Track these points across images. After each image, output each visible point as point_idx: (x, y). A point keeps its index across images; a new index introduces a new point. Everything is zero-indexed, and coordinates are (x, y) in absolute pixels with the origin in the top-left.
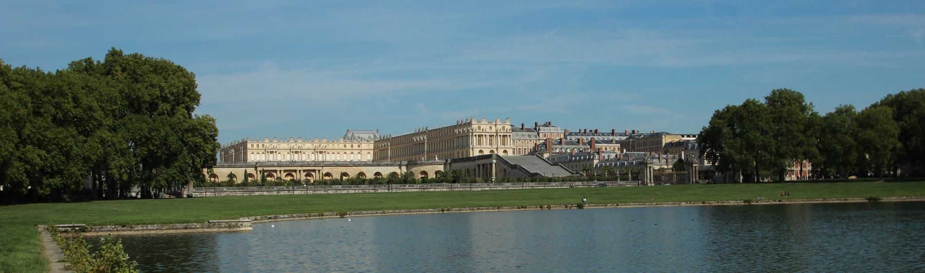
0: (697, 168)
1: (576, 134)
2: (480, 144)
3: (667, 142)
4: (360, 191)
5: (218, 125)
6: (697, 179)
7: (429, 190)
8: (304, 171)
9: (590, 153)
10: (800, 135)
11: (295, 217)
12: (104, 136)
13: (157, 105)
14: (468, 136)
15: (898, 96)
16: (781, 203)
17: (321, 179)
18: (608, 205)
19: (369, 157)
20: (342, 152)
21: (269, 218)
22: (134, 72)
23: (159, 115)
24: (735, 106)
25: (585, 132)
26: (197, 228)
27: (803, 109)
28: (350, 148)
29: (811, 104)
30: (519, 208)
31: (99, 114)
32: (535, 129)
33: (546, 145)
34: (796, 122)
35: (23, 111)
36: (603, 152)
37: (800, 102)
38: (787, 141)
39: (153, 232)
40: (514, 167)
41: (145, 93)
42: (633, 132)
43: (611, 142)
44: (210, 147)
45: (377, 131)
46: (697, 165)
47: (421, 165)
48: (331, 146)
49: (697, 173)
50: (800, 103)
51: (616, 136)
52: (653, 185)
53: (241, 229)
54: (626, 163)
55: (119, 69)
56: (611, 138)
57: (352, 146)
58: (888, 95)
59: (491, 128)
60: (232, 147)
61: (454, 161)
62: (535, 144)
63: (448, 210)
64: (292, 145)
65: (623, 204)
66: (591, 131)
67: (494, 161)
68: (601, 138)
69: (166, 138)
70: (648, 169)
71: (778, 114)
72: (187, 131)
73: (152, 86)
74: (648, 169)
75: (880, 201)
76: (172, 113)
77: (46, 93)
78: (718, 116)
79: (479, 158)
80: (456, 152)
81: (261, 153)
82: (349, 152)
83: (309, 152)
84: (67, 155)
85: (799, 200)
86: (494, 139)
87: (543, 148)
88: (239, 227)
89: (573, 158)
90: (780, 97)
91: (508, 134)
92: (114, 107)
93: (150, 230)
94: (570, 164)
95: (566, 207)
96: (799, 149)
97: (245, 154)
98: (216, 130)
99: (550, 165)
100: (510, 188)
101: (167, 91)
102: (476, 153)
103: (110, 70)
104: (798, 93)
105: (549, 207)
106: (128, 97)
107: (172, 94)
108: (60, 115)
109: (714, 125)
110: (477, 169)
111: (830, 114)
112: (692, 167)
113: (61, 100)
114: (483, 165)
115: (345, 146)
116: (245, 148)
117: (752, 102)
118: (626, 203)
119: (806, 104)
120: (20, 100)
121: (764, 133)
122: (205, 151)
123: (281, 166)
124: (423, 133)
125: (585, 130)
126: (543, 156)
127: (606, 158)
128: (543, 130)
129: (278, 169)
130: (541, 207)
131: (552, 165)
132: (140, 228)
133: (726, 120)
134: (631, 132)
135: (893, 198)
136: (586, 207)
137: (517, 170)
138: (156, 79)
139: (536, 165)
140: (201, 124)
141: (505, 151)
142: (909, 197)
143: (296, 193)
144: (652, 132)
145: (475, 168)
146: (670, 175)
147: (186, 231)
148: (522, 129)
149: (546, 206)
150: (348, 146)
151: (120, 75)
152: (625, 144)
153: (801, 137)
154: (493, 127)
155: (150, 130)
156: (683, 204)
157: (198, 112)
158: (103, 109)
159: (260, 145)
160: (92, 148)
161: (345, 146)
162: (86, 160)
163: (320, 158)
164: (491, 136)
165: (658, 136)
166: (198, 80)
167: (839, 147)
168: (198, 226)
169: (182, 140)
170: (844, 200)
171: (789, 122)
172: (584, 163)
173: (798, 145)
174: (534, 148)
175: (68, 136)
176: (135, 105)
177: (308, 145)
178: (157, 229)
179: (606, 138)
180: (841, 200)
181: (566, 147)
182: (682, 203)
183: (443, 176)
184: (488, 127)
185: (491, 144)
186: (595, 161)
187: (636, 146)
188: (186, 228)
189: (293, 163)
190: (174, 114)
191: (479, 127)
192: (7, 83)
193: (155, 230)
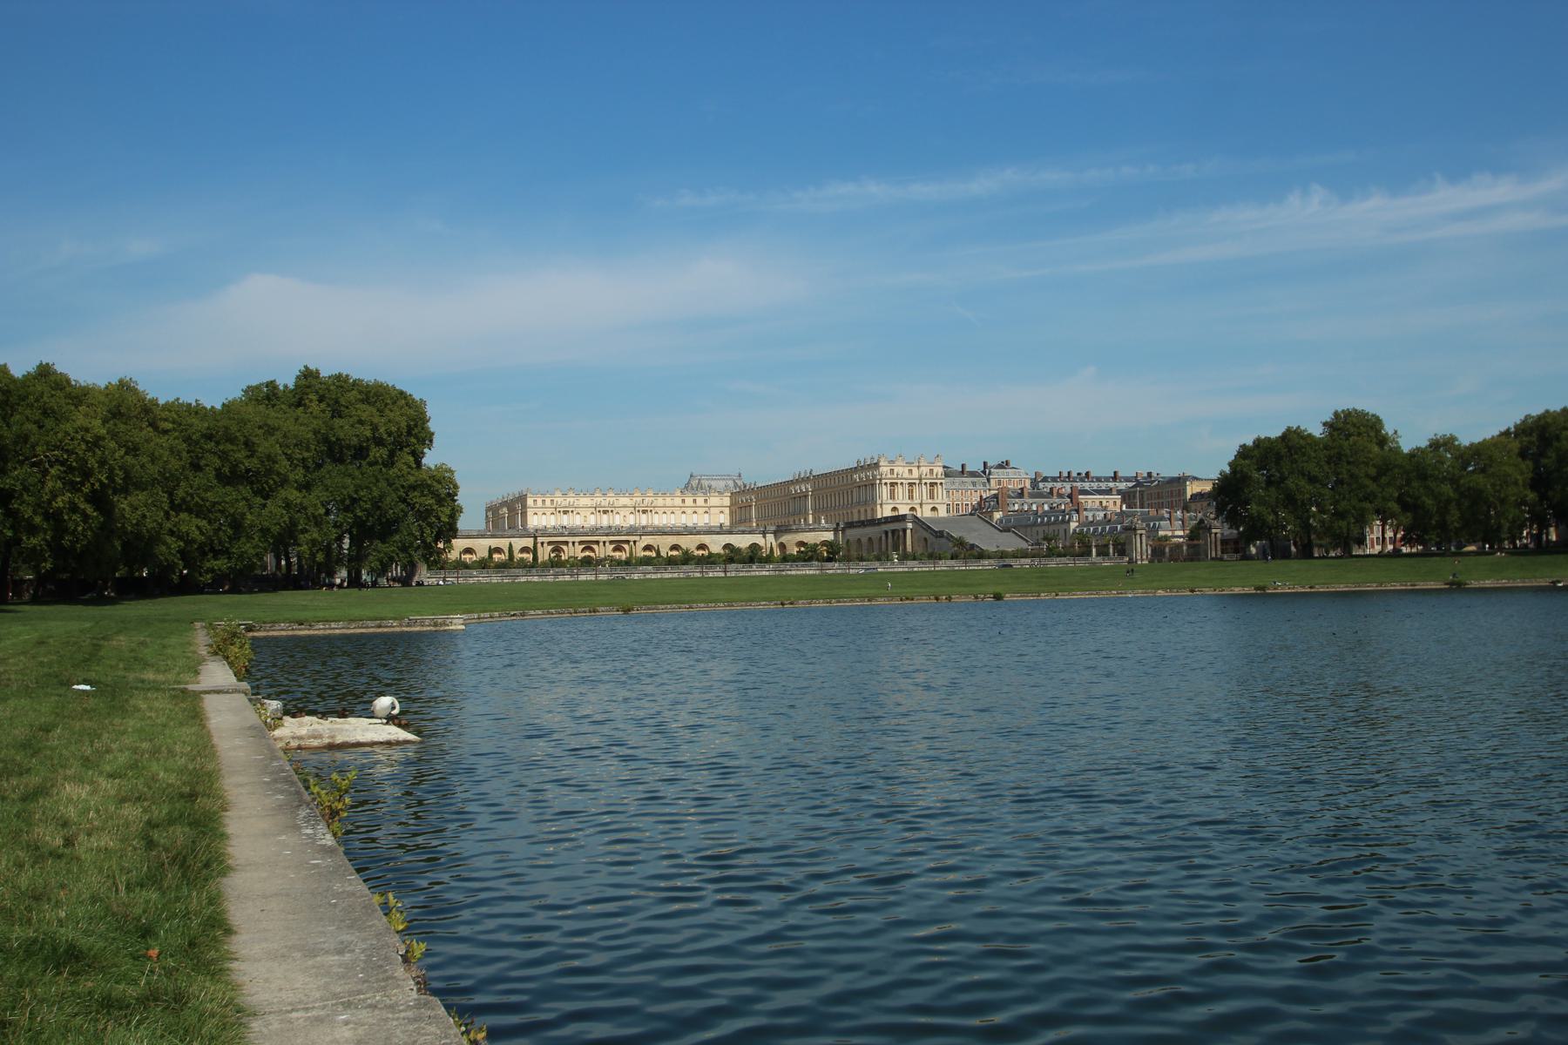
0: (1219, 535)
1: (1054, 479)
2: (892, 496)
3: (1194, 492)
4: (682, 575)
5: (458, 478)
6: (1219, 553)
7: (789, 573)
9: (1064, 511)
10: (1368, 482)
11: (552, 614)
12: (291, 498)
13: (368, 449)
14: (873, 485)
15: (1540, 418)
16: (1313, 590)
17: (399, 574)
18: (1042, 594)
19: (724, 519)
20: (678, 511)
21: (514, 615)
22: (337, 402)
23: (371, 464)
24: (1269, 438)
25: (1069, 477)
26: (393, 627)
27: (1382, 441)
28: (692, 504)
29: (1396, 432)
30: (901, 600)
31: (283, 465)
32: (984, 472)
33: (997, 498)
34: (1364, 462)
35: (175, 464)
36: (1086, 510)
37: (1376, 430)
38: (1350, 492)
39: (337, 631)
40: (940, 535)
42: (1150, 474)
43: (1109, 492)
44: (447, 511)
45: (740, 476)
46: (1218, 531)
47: (797, 531)
48: (660, 502)
49: (1219, 543)
50: (1378, 431)
51: (1121, 481)
52: (1146, 562)
53: (451, 628)
54: (1119, 527)
55: (313, 397)
56: (1111, 485)
57: (695, 501)
58: (1526, 417)
59: (910, 471)
60: (504, 504)
61: (850, 525)
62: (981, 496)
63: (791, 604)
64: (598, 500)
65: (1066, 593)
66: (1079, 474)
67: (910, 525)
68: (1095, 485)
69: (381, 497)
70: (1138, 537)
71: (1336, 451)
72: (413, 488)
73: (361, 422)
74: (1138, 537)
75: (1467, 586)
76: (390, 462)
77: (209, 437)
78: (1244, 453)
79: (887, 520)
80: (855, 511)
81: (548, 513)
82: (689, 511)
83: (623, 512)
84: (237, 525)
85: (1342, 586)
86: (916, 490)
87: (992, 503)
88: (448, 625)
89: (1039, 520)
90: (1345, 423)
91: (939, 481)
92: (306, 455)
93: (334, 629)
94: (1035, 529)
95: (976, 598)
96: (1367, 505)
97: (524, 514)
98: (456, 487)
99: (997, 532)
100: (915, 569)
101: (382, 430)
102: (887, 512)
103: (301, 399)
104: (1373, 415)
105: (949, 599)
106: (326, 440)
107: (390, 434)
108: (226, 470)
109: (1235, 469)
110: (884, 538)
111: (1418, 449)
112: (1211, 534)
113: (229, 447)
114: (893, 532)
115: (683, 501)
116: (524, 506)
117: (1295, 431)
118: (1070, 591)
119: (1387, 434)
120: (171, 450)
121: (1312, 480)
122: (438, 518)
123: (574, 535)
124: (806, 480)
125: (1069, 473)
126: (991, 517)
127: (1091, 519)
128: (997, 474)
129: (570, 539)
130: (937, 599)
131: (1001, 531)
132: (321, 627)
133: (1254, 461)
134: (1146, 475)
135: (1487, 582)
136: (1007, 597)
137: (943, 540)
138: (366, 412)
139: (975, 531)
140: (432, 477)
141: (934, 509)
142: (1511, 581)
143: (582, 578)
144: (1182, 475)
145: (881, 538)
146: (1179, 546)
147: (380, 630)
148: (963, 472)
149: (944, 597)
150: (689, 501)
151: (315, 407)
152: (1129, 496)
153: (1372, 487)
154: (915, 470)
155: (358, 488)
156: (1160, 592)
157: (431, 459)
158: (289, 458)
159: (548, 503)
160: (272, 513)
161: (683, 501)
162: (265, 532)
163: (644, 520)
164: (911, 484)
165: (1180, 481)
166: (430, 411)
167: (1429, 502)
168: (395, 624)
169: (404, 501)
170: (1412, 585)
171: (1353, 462)
172: (1046, 528)
173: (1365, 499)
174: (979, 504)
175: (235, 498)
176: (335, 451)
177: (624, 501)
178: (343, 628)
179: (1103, 486)
180: (1406, 585)
181: (1030, 501)
182: (1159, 591)
183: (811, 551)
184: (906, 470)
185: (911, 497)
186: (1072, 524)
187: (1145, 499)
188: (380, 627)
189: (595, 531)
190: (393, 464)
191: (892, 471)
192: (153, 425)
193: (340, 629)
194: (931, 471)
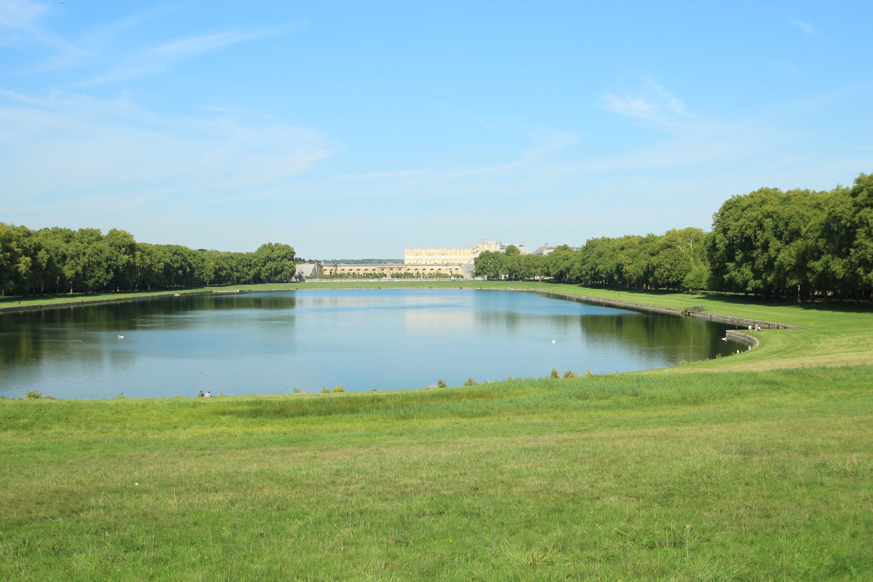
8: (398, 268)
41: (274, 255)
45: (499, 240)
48: (448, 251)
59: (489, 248)
64: (428, 251)
84: (247, 274)
136: (382, 288)
150: (458, 251)
160: (252, 272)
175: (245, 269)
176: (269, 259)
177: (436, 251)
191: (483, 248)
194: (496, 248)
